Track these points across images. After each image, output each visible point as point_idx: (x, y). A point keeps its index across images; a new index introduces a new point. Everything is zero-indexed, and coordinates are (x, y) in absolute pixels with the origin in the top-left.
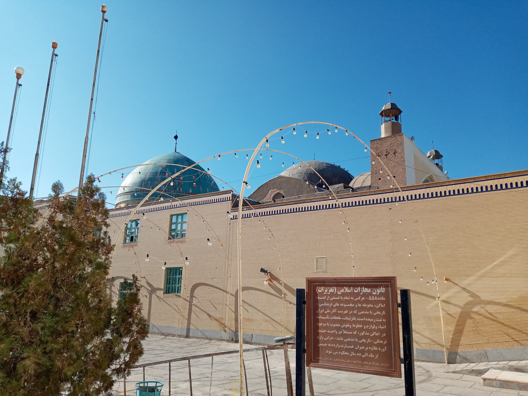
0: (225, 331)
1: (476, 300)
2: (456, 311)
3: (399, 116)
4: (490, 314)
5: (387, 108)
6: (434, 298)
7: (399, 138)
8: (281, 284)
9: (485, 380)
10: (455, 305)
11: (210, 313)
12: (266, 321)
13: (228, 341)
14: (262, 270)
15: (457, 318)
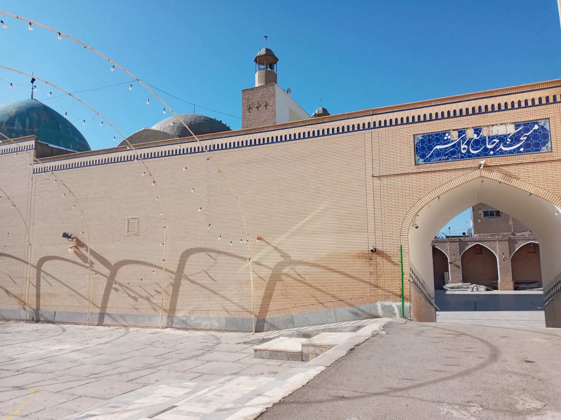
0: (25, 309)
1: (287, 261)
2: (266, 273)
3: (275, 65)
4: (299, 275)
6: (244, 259)
7: (271, 88)
8: (87, 250)
9: (256, 351)
11: (8, 289)
12: (71, 295)
13: (27, 321)
14: (65, 235)
15: (267, 280)
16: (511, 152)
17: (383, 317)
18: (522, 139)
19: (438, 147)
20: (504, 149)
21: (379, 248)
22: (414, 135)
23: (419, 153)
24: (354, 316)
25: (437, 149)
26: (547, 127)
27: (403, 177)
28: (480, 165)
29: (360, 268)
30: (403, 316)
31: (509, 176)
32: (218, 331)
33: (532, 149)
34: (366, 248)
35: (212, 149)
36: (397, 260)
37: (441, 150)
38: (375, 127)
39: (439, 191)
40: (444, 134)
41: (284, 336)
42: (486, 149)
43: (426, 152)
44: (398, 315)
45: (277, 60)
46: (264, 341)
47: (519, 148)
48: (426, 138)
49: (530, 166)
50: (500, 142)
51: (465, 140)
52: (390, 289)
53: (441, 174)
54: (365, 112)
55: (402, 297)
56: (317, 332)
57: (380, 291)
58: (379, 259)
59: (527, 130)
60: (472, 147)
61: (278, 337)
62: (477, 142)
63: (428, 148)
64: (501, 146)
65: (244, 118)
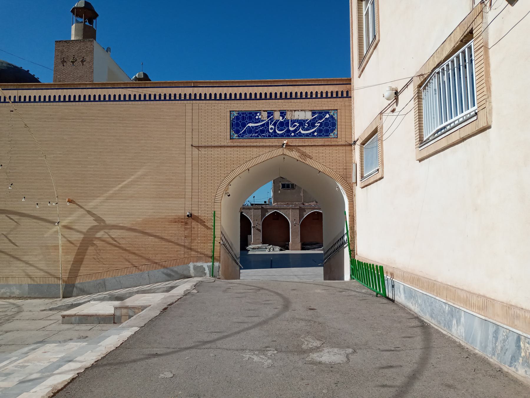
1: (101, 224)
2: (77, 237)
3: (94, 21)
4: (113, 239)
5: (79, 6)
6: (53, 223)
7: (89, 44)
9: (64, 317)
10: (78, 231)
16: (307, 135)
17: (195, 276)
18: (316, 125)
19: (250, 125)
20: (303, 132)
21: (195, 213)
22: (230, 111)
23: (234, 128)
24: (167, 278)
25: (249, 126)
26: (335, 116)
27: (219, 149)
28: (283, 145)
29: (175, 232)
30: (213, 275)
31: (304, 155)
32: (19, 298)
33: (323, 134)
34: (183, 213)
35: (17, 100)
36: (210, 224)
37: (253, 127)
38: (195, 99)
39: (249, 165)
40: (257, 113)
41: (95, 300)
42: (289, 131)
43: (240, 128)
44: (208, 275)
45: (98, 15)
46: (73, 306)
47: (313, 132)
48: (240, 115)
49: (321, 149)
50: (299, 126)
51: (272, 121)
52: (203, 251)
53: (251, 149)
54: (187, 83)
55: (213, 258)
56: (131, 294)
57: (193, 253)
58: (194, 224)
59: (321, 118)
60: (278, 128)
61: (89, 301)
62: (282, 124)
63: (241, 124)
64: (300, 130)
65: (56, 71)
